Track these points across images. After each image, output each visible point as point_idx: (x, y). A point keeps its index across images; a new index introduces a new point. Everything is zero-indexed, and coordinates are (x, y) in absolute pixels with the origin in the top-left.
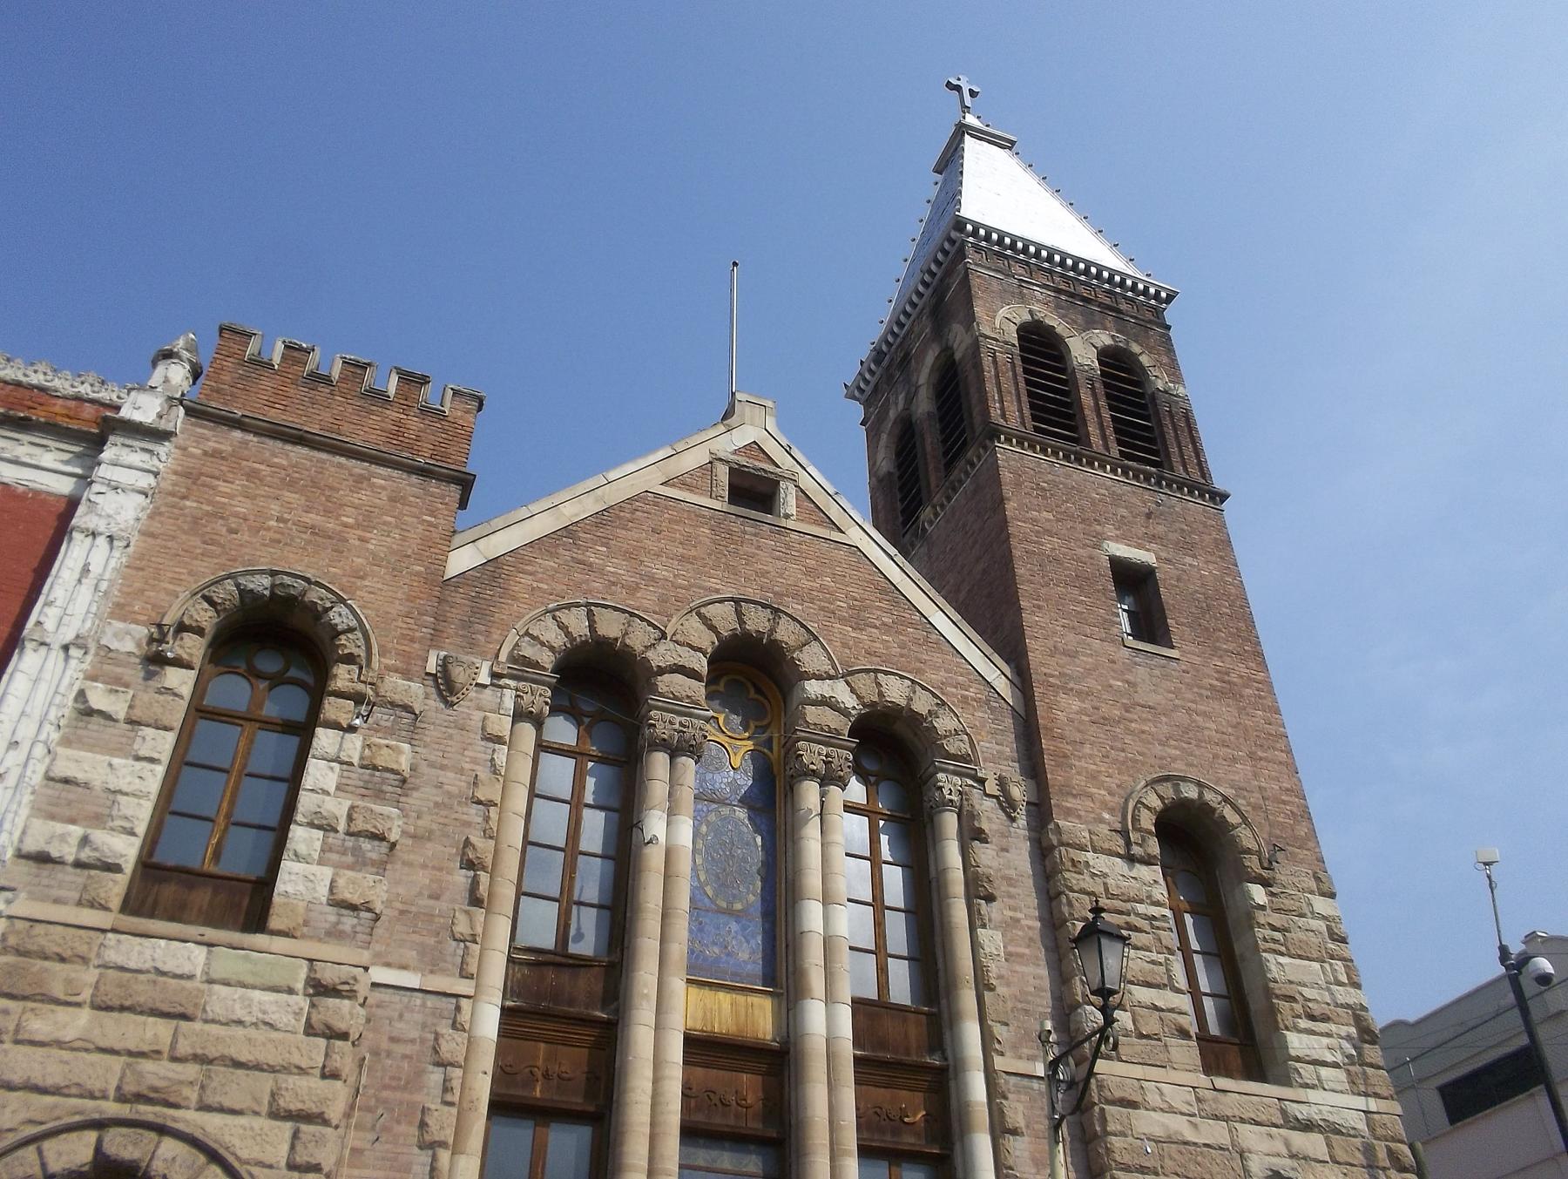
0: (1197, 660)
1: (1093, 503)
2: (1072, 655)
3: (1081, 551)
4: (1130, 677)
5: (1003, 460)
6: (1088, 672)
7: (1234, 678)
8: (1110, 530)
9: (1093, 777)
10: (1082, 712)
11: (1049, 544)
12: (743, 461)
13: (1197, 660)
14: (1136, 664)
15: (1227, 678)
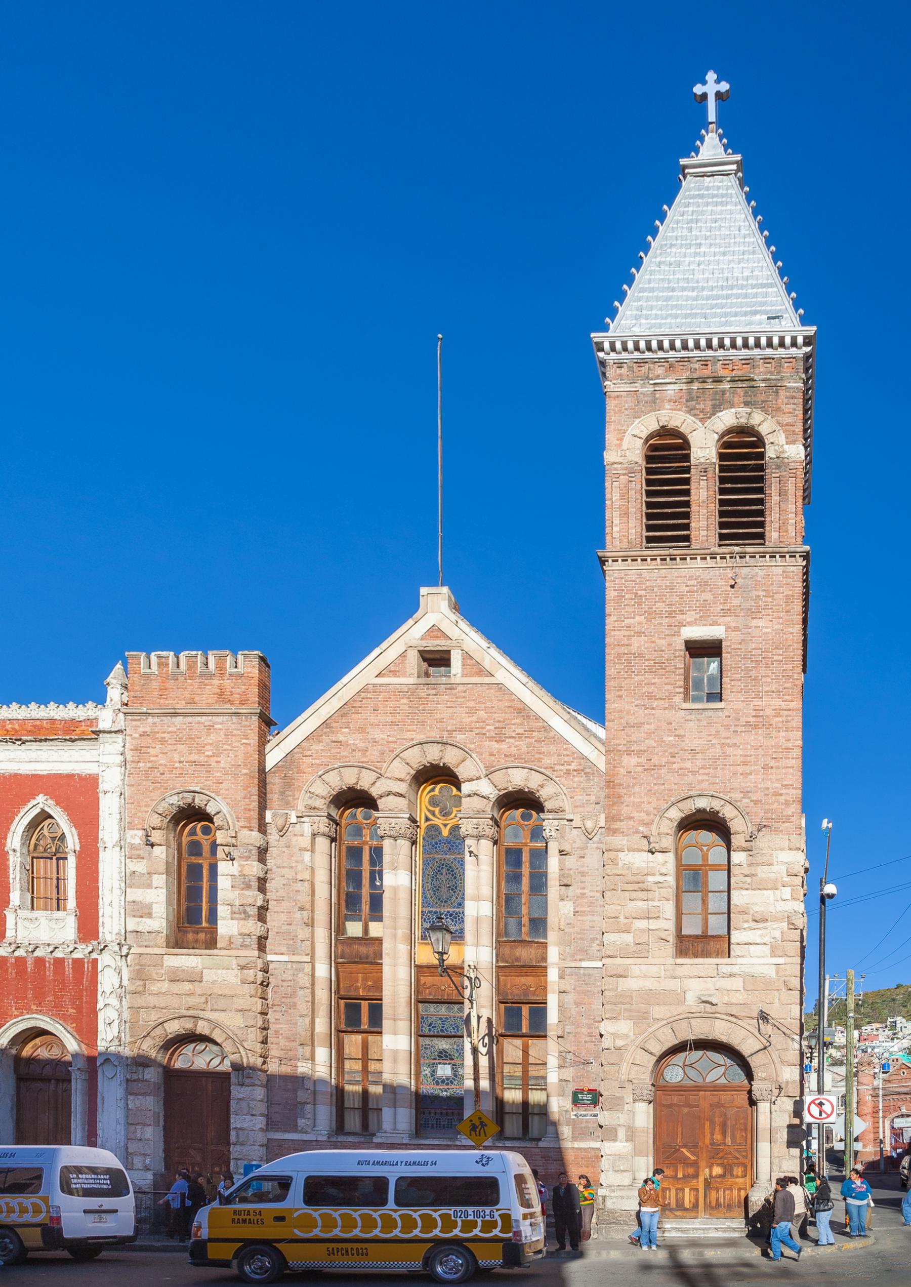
0: (740, 705)
1: (682, 597)
2: (639, 725)
3: (663, 642)
4: (681, 732)
5: (611, 581)
6: (649, 734)
7: (768, 712)
8: (690, 616)
9: (638, 806)
10: (639, 765)
11: (637, 643)
12: (424, 643)
13: (740, 705)
14: (688, 720)
15: (761, 713)
